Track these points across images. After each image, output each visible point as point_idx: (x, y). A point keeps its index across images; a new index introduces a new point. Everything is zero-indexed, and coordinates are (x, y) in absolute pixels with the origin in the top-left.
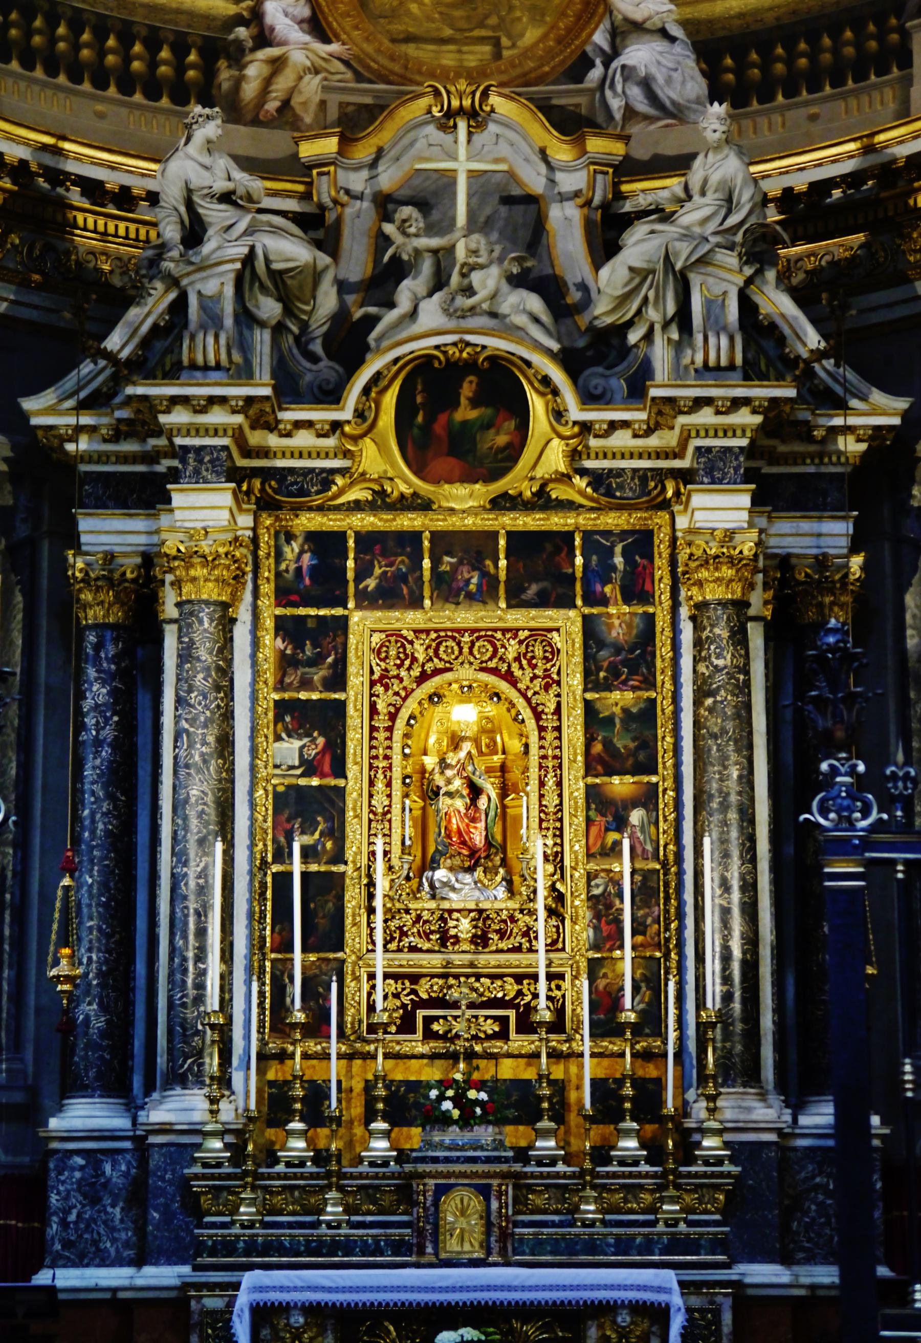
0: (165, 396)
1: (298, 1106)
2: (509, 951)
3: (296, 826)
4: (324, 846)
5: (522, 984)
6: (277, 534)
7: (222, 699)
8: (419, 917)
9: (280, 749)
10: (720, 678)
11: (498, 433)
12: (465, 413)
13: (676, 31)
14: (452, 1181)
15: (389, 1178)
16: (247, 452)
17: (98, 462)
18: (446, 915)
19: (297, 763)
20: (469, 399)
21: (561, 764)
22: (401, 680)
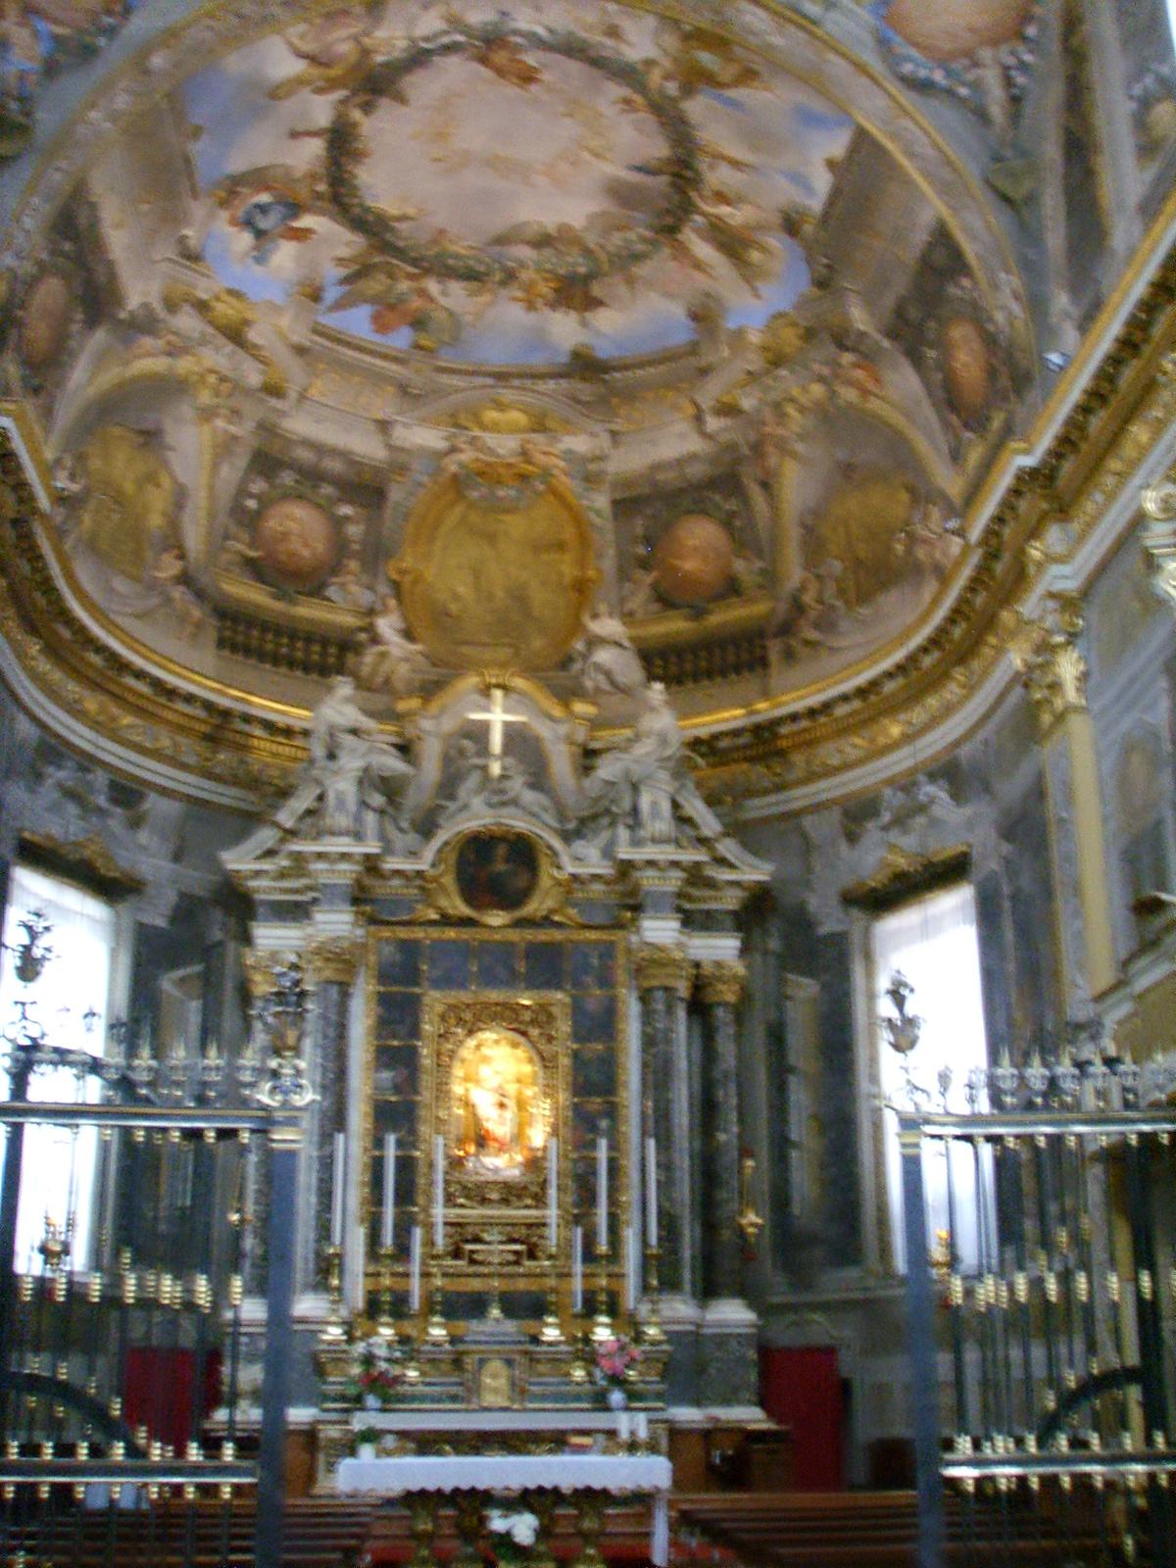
1: (387, 1307)
13: (626, 643)
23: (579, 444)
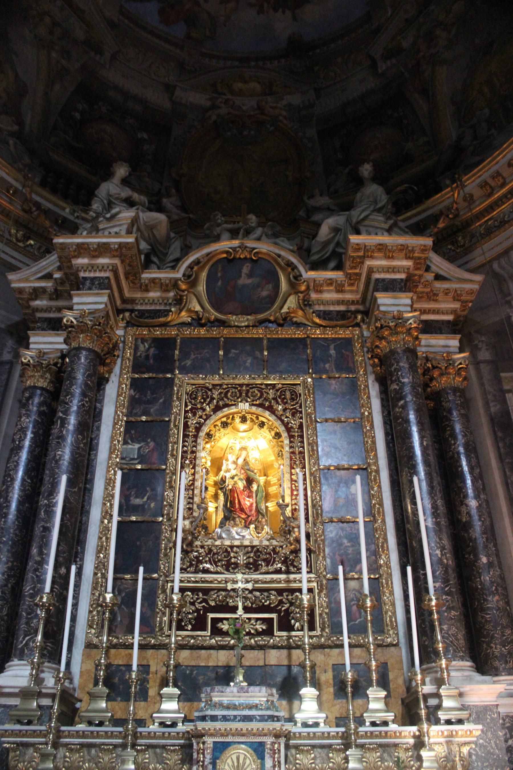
0: (74, 243)
2: (272, 573)
3: (133, 493)
4: (149, 505)
5: (282, 595)
6: (136, 339)
7: (87, 402)
8: (210, 550)
9: (126, 448)
10: (407, 389)
11: (262, 291)
12: (244, 281)
13: (333, 207)
14: (229, 739)
15: (174, 738)
16: (124, 301)
17: (45, 311)
18: (229, 549)
19: (136, 457)
20: (246, 274)
21: (304, 456)
22: (204, 410)
23: (296, 99)
